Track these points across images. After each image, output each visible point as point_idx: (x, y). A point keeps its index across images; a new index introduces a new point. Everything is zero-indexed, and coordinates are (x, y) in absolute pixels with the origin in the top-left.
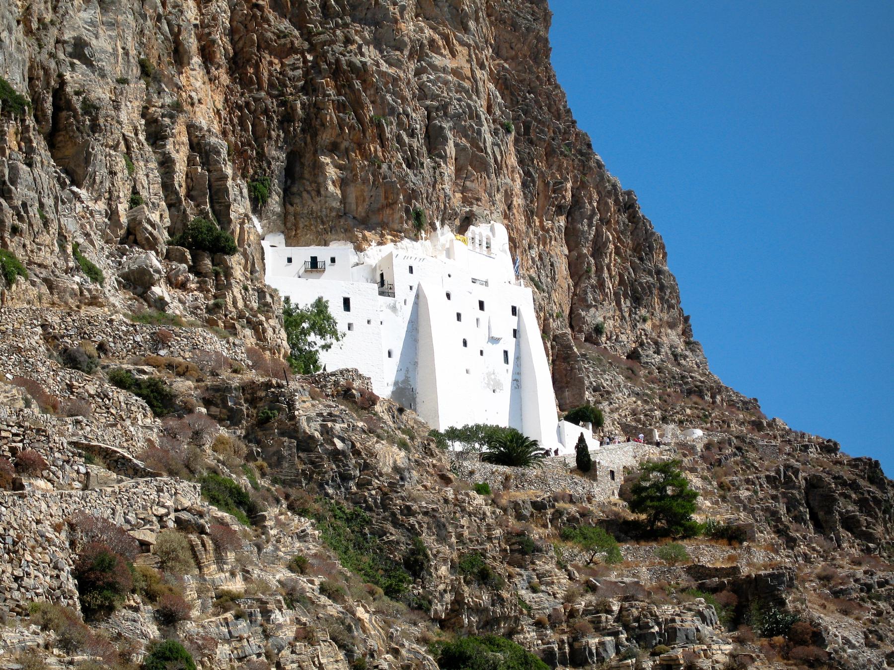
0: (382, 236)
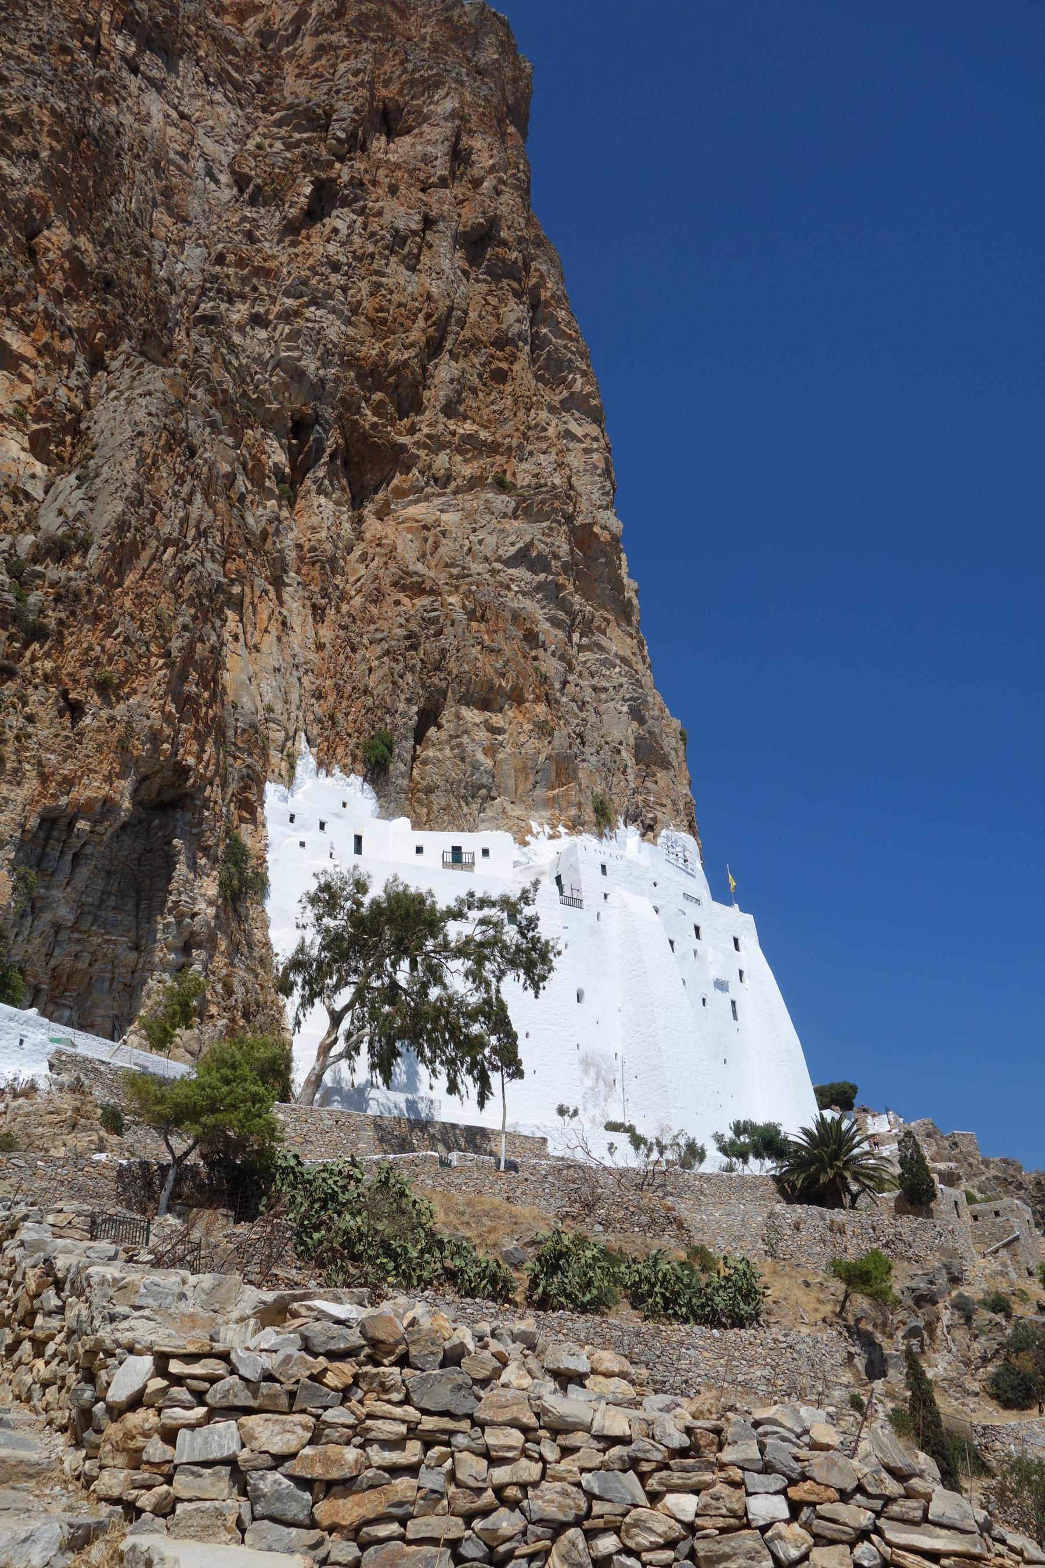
0: (553, 827)
